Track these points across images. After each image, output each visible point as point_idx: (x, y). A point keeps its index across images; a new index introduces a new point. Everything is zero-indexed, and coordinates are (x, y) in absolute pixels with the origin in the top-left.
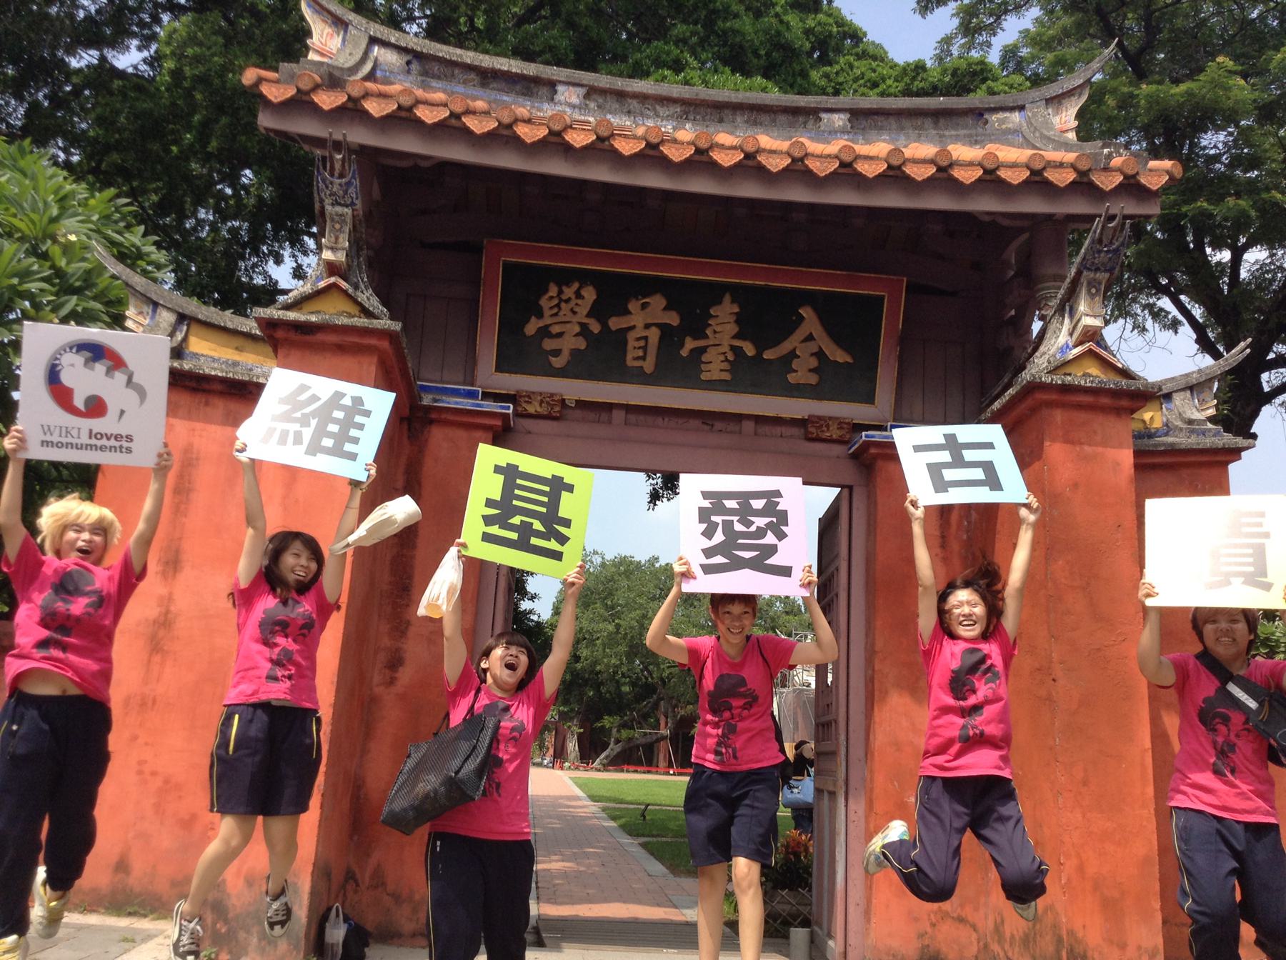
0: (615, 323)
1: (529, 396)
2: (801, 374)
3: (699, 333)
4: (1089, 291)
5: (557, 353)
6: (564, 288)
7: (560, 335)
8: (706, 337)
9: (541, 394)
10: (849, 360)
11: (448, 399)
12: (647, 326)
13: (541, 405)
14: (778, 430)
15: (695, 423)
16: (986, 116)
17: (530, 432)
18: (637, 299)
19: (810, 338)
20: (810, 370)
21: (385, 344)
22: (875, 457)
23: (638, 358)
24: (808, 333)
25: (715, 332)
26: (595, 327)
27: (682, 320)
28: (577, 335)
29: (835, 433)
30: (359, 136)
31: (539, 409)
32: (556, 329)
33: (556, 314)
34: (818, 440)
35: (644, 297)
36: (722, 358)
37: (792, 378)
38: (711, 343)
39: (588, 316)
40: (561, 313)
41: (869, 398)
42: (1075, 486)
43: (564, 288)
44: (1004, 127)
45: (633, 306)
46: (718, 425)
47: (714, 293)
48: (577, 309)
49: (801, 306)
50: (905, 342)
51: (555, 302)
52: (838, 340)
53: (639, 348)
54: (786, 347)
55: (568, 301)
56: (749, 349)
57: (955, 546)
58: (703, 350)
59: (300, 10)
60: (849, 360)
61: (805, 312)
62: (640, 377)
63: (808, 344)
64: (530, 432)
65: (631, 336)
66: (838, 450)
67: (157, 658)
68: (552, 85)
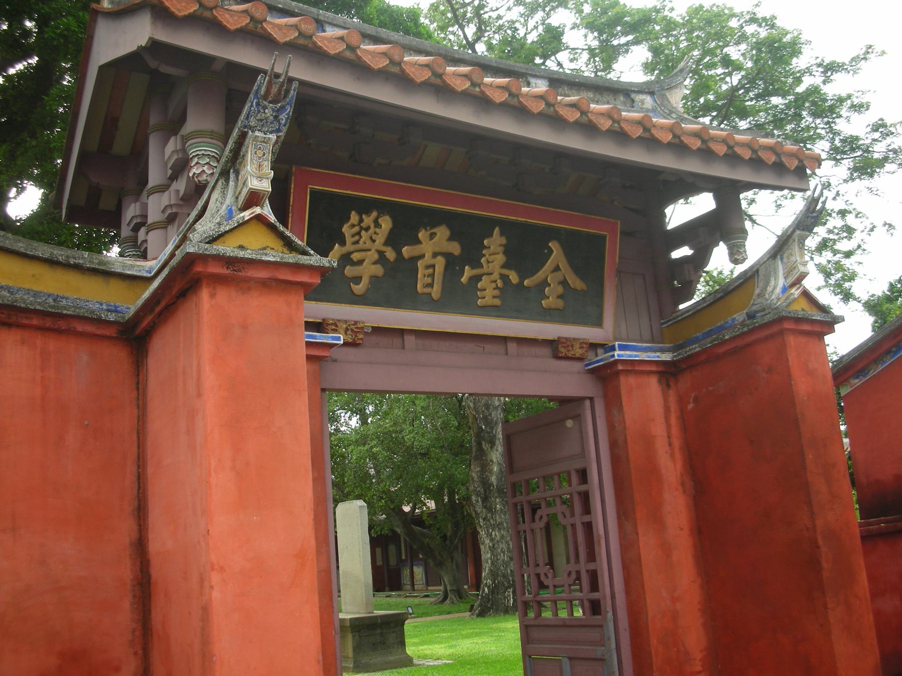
0: (406, 251)
3: (476, 264)
6: (364, 216)
7: (360, 262)
9: (346, 322)
12: (435, 255)
15: (470, 346)
17: (335, 361)
19: (557, 269)
20: (559, 297)
22: (618, 373)
26: (391, 254)
27: (462, 250)
29: (578, 352)
32: (355, 256)
33: (357, 242)
34: (566, 358)
36: (494, 285)
38: (485, 269)
39: (386, 243)
40: (362, 240)
43: (364, 216)
45: (422, 235)
47: (486, 226)
51: (357, 229)
52: (578, 270)
53: (428, 276)
54: (540, 275)
55: (367, 229)
56: (514, 277)
57: (677, 443)
58: (478, 278)
63: (556, 274)
64: (335, 361)
65: (421, 264)
66: (577, 366)
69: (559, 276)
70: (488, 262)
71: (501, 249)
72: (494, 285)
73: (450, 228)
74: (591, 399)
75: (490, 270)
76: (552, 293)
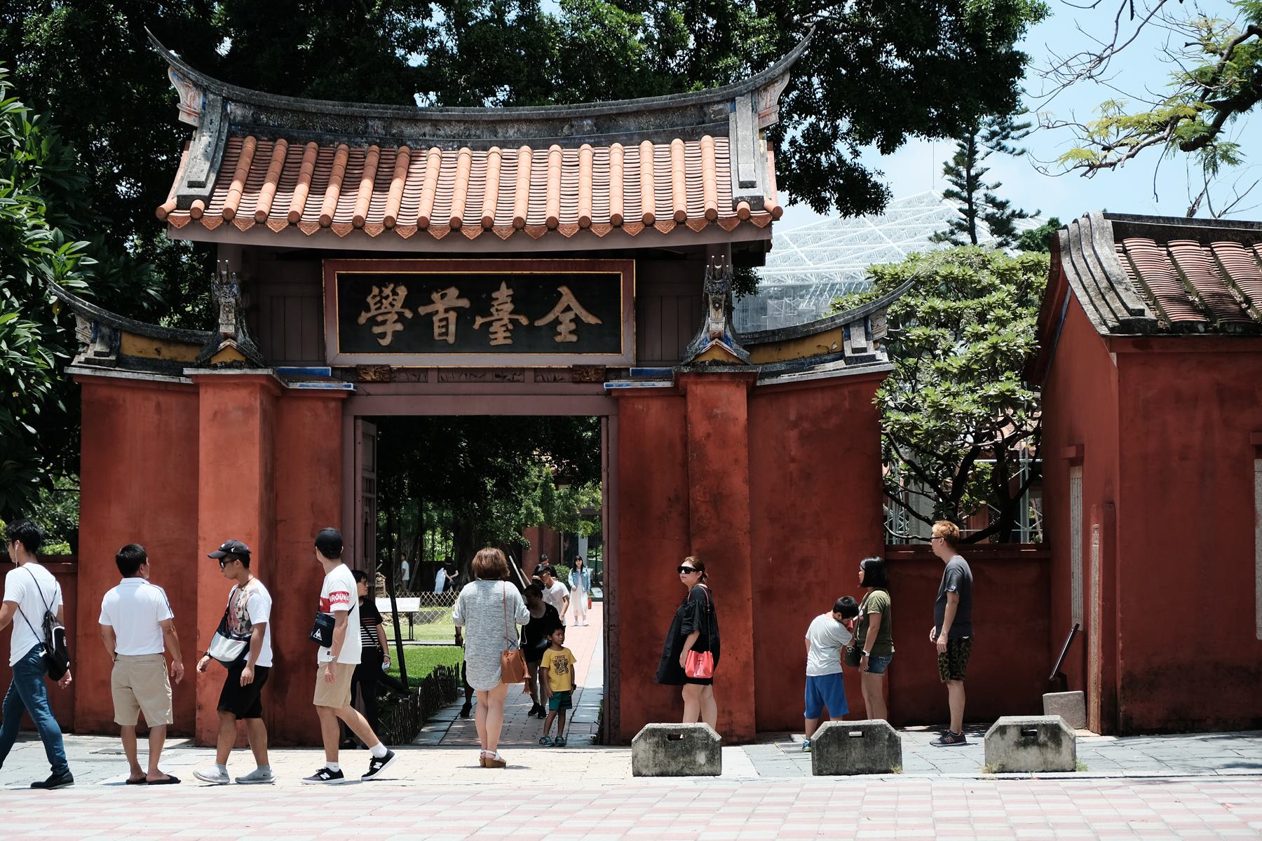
0: (423, 310)
1: (365, 368)
2: (565, 331)
4: (714, 307)
5: (383, 335)
8: (492, 315)
9: (374, 366)
10: (600, 322)
11: (309, 384)
12: (447, 311)
13: (375, 375)
16: (705, 109)
17: (369, 394)
18: (437, 292)
19: (568, 309)
20: (571, 332)
21: (264, 382)
23: (440, 335)
24: (566, 305)
25: (497, 310)
26: (409, 314)
28: (395, 322)
31: (374, 377)
32: (380, 319)
34: (580, 382)
35: (443, 290)
36: (504, 329)
37: (558, 339)
38: (496, 317)
39: (401, 307)
40: (383, 307)
42: (709, 435)
44: (717, 117)
48: (394, 303)
49: (560, 285)
51: (378, 299)
53: (443, 327)
54: (550, 317)
56: (524, 321)
58: (490, 324)
59: (167, 74)
60: (600, 322)
61: (564, 290)
62: (445, 348)
64: (369, 394)
65: (435, 319)
69: (571, 315)
70: (497, 310)
71: (509, 300)
72: (504, 329)
73: (457, 287)
74: (607, 417)
75: (498, 317)
76: (565, 328)
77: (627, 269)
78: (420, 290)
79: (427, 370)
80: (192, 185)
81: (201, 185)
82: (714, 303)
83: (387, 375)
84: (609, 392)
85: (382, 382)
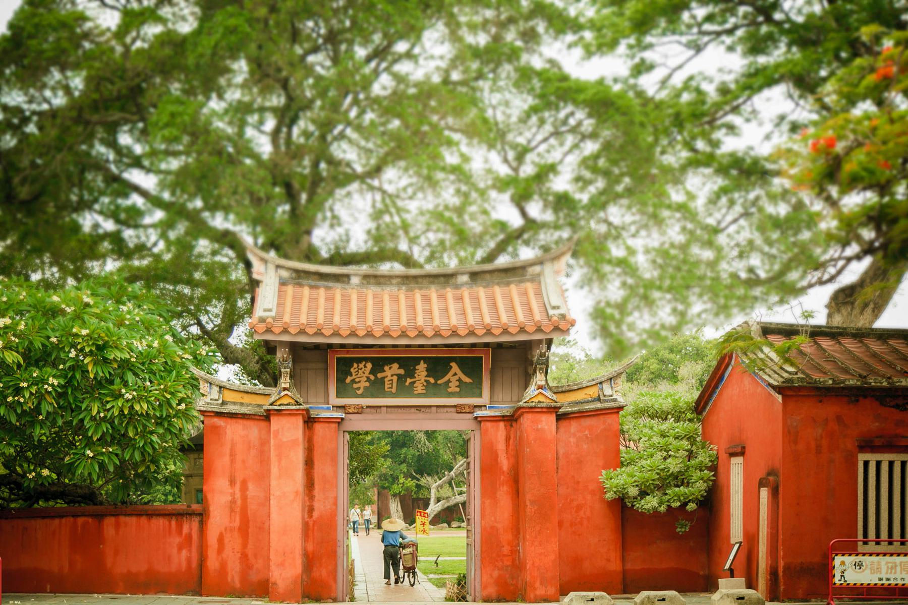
0: (380, 375)
1: (350, 406)
2: (453, 387)
3: (412, 376)
5: (359, 389)
10: (471, 381)
12: (392, 376)
14: (446, 409)
15: (413, 410)
19: (455, 374)
26: (372, 378)
30: (286, 338)
32: (357, 380)
37: (449, 390)
39: (369, 374)
41: (480, 396)
45: (386, 368)
46: (423, 410)
50: (492, 373)
56: (432, 380)
58: (414, 382)
60: (471, 381)
61: (453, 364)
65: (386, 380)
66: (469, 416)
67: (233, 514)
68: (348, 276)
69: (456, 378)
73: (398, 363)
77: (487, 354)
78: (379, 364)
79: (381, 407)
80: (265, 310)
81: (270, 310)
82: (540, 370)
83: (360, 410)
84: (476, 418)
85: (357, 413)
